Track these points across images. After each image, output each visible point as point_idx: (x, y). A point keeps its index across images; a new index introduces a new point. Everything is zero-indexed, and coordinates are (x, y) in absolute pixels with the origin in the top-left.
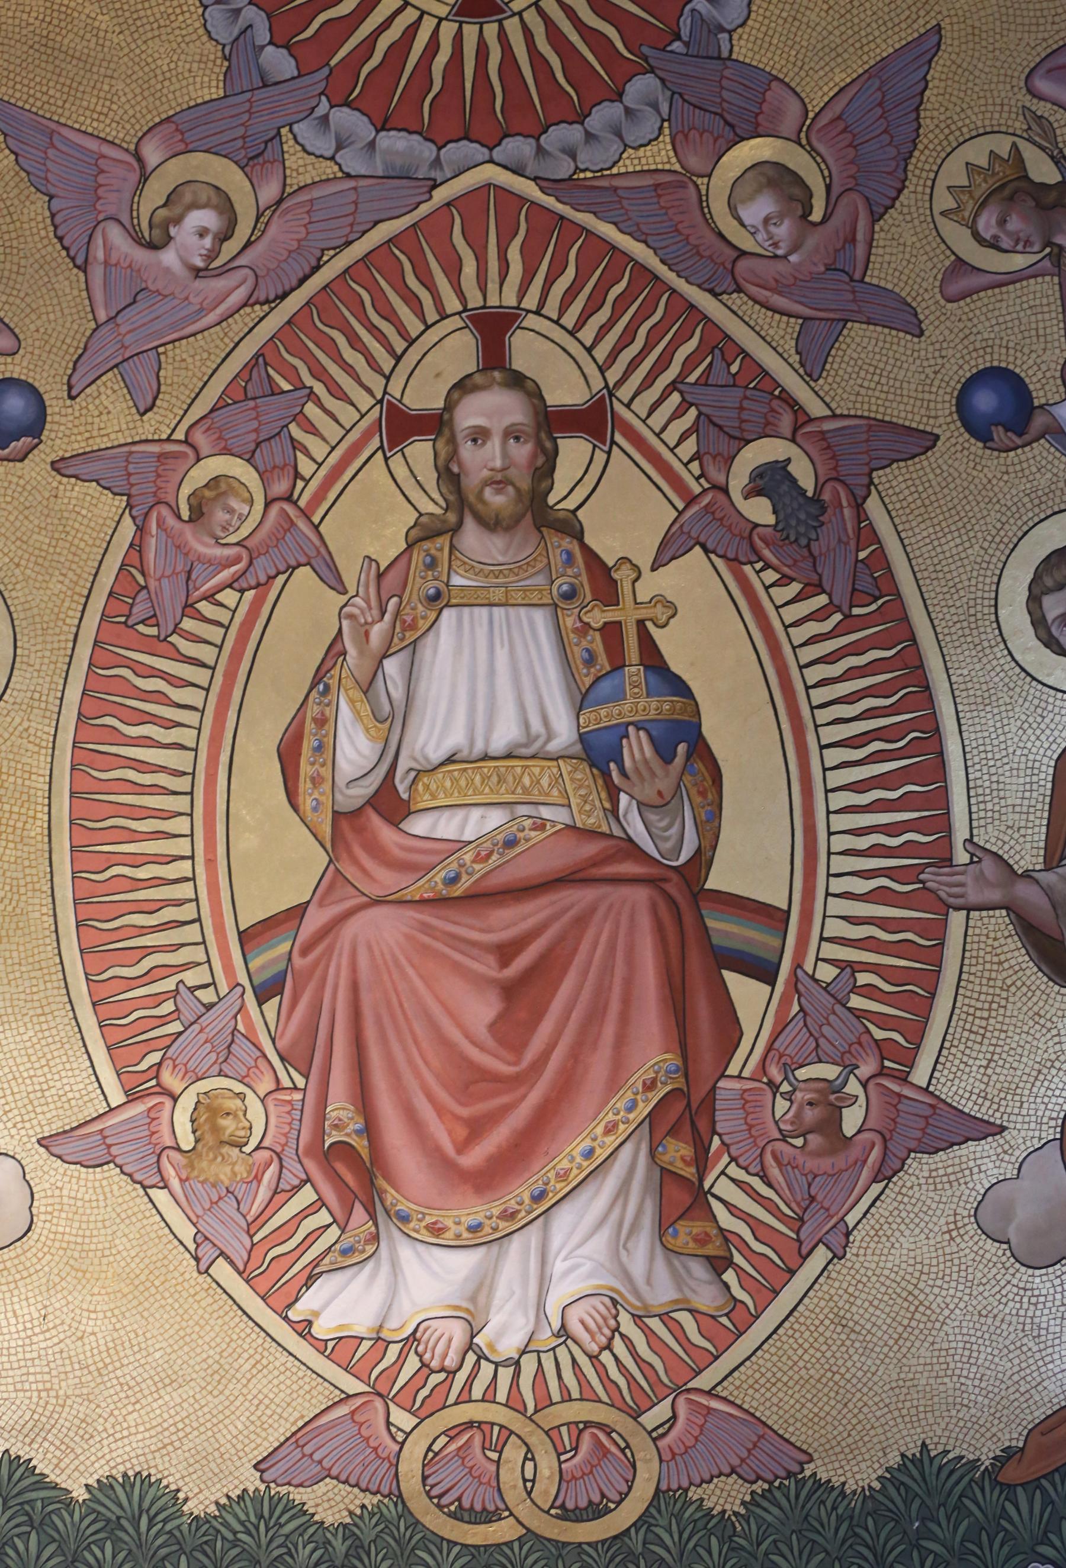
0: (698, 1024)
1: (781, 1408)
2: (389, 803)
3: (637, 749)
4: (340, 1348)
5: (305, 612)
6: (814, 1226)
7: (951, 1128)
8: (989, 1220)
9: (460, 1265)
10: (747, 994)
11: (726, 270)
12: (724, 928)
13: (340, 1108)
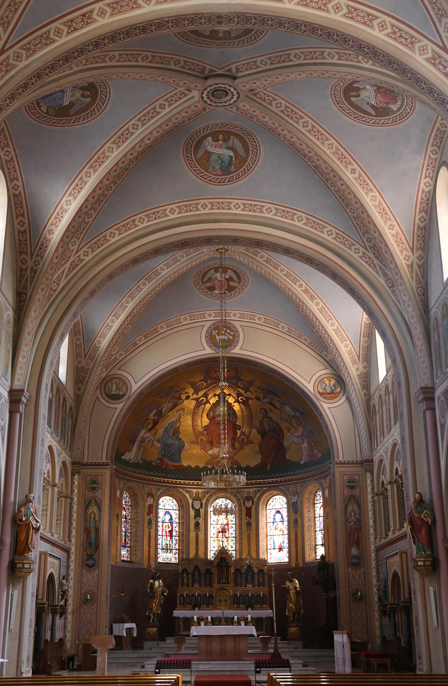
2: (214, 418)
3: (231, 414)
4: (210, 455)
5: (208, 406)
6: (242, 448)
7: (251, 442)
9: (218, 449)
10: (238, 431)
11: (240, 388)
12: (237, 427)
13: (210, 438)
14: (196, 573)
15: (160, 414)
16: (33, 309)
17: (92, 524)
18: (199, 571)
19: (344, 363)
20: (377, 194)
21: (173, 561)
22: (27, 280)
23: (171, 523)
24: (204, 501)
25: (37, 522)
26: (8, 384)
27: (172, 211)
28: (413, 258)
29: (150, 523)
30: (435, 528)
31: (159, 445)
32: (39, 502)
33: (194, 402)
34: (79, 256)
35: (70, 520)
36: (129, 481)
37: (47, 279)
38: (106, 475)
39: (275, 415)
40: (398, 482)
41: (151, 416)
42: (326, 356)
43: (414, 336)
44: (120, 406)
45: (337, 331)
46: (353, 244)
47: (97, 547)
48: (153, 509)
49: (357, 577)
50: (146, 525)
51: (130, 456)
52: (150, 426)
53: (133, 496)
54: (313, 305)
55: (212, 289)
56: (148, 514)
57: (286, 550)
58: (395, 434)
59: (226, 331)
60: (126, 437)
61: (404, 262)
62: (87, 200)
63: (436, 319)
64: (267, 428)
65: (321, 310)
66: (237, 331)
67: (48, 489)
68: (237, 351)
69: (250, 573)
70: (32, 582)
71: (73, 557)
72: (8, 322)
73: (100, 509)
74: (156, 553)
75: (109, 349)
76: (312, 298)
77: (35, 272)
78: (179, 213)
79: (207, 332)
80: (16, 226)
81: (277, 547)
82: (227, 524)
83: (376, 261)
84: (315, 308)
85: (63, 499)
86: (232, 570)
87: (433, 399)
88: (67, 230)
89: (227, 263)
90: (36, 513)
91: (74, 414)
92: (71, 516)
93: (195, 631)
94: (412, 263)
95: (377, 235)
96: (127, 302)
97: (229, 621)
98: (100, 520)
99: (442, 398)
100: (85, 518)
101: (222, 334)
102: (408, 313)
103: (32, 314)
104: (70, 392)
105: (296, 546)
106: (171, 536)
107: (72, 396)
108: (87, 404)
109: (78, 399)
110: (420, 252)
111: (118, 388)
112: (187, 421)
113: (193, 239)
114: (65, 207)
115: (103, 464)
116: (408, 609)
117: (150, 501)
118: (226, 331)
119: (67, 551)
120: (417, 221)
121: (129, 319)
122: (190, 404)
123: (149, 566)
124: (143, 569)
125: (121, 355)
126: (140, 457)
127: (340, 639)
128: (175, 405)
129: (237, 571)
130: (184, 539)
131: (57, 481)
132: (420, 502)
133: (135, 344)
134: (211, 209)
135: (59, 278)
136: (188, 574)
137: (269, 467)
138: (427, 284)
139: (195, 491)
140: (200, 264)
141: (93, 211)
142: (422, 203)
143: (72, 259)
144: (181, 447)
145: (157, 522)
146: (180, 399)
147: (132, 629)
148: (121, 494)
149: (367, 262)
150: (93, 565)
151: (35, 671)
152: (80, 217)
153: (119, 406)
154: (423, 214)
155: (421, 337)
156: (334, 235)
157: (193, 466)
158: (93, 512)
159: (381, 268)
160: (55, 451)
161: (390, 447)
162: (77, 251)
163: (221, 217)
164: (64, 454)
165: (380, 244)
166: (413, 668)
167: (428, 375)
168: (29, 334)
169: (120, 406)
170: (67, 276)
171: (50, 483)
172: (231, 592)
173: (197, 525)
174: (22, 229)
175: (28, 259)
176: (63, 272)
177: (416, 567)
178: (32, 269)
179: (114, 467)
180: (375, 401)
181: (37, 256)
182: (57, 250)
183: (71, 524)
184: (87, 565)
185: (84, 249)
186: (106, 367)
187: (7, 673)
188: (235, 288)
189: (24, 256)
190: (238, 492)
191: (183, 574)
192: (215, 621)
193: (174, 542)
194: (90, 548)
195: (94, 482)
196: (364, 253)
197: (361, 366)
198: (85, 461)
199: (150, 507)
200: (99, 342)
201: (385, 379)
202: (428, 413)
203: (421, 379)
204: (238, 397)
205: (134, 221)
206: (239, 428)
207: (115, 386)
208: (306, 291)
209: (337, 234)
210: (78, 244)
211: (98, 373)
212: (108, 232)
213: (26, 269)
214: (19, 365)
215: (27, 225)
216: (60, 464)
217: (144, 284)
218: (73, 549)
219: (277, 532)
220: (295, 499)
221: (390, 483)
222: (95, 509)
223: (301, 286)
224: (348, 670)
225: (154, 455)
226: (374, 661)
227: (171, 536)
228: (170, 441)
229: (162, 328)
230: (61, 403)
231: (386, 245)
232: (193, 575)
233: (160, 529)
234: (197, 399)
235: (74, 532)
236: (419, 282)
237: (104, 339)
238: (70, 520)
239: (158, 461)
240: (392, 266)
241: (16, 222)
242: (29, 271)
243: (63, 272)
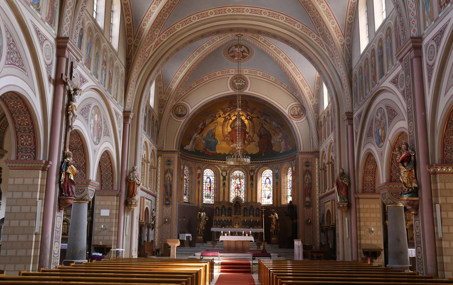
0: (245, 136)
1: (247, 151)
2: (234, 127)
5: (231, 121)
6: (249, 144)
7: (253, 141)
8: (255, 145)
14: (223, 209)
15: (204, 125)
16: (135, 67)
17: (168, 183)
18: (225, 208)
19: (305, 99)
20: (325, 4)
21: (211, 203)
22: (132, 51)
23: (210, 183)
24: (228, 172)
25: (139, 181)
26: (123, 108)
27: (211, 13)
28: (344, 41)
29: (199, 183)
30: (350, 187)
31: (204, 142)
32: (139, 171)
33: (223, 119)
34: (160, 38)
35: (156, 181)
36: (188, 160)
37: (143, 51)
38: (175, 157)
39: (267, 127)
40: (332, 163)
41: (200, 126)
42: (296, 94)
43: (343, 84)
44: (183, 121)
45: (302, 81)
46: (312, 33)
47: (171, 195)
48: (200, 176)
49: (308, 212)
50: (197, 184)
51: (188, 147)
52: (199, 132)
53: (190, 169)
54: (289, 66)
55: (234, 57)
56: (198, 178)
57: (271, 198)
58: (331, 137)
59: (241, 81)
60: (186, 138)
61: (339, 43)
62: (164, 7)
63: (355, 75)
64: (262, 134)
65: (293, 69)
66: (247, 80)
67: (145, 165)
68: (247, 91)
69: (252, 210)
70: (137, 211)
71: (158, 200)
72: (122, 75)
73: (172, 175)
74: (202, 199)
75: (177, 90)
76: (289, 62)
77: (136, 47)
78: (215, 14)
79: (231, 81)
80: (126, 21)
81: (267, 196)
82: (240, 184)
83: (324, 42)
84: (290, 68)
85: (153, 169)
86: (242, 208)
87: (352, 119)
88: (153, 24)
89: (242, 42)
90: (138, 176)
91: (158, 124)
92: (157, 178)
93: (222, 238)
94: (344, 44)
95: (324, 28)
96: (187, 64)
97: (240, 234)
98: (172, 181)
99: (357, 118)
100: (165, 180)
101: (239, 82)
102: (340, 71)
103: (135, 70)
104: (156, 112)
105: (277, 196)
106: (210, 190)
107: (157, 115)
108: (165, 119)
109: (161, 117)
110: (348, 37)
111: (182, 111)
112: (219, 129)
113: (223, 29)
114: (152, 11)
115: (174, 152)
116: (334, 229)
117: (199, 171)
118: (241, 81)
119: (155, 196)
120: (347, 20)
121: (188, 73)
122: (221, 120)
123: (199, 205)
124: (195, 207)
125: (183, 93)
126: (194, 148)
127: (297, 243)
128: (213, 120)
129: (245, 208)
130: (217, 191)
131: (149, 160)
132: (342, 174)
133: (191, 87)
134: (233, 12)
135: (149, 51)
136: (219, 210)
137: (263, 154)
138: (351, 55)
139: (223, 166)
140: (227, 43)
141: (167, 13)
142: (350, 9)
143: (156, 40)
144: (216, 143)
145: (203, 182)
146: (216, 117)
147: (190, 237)
148: (184, 168)
149: (319, 43)
150: (169, 204)
151: (139, 255)
152: (160, 16)
153: (183, 121)
154: (351, 16)
155: (347, 85)
156: (301, 28)
157: (222, 153)
158: (169, 176)
159: (326, 46)
160: (148, 144)
161: (329, 144)
162: (159, 36)
163: (238, 17)
164: (153, 146)
165: (326, 33)
166: (335, 258)
167: (350, 106)
168: (133, 81)
169: (183, 121)
170: (153, 49)
171: (145, 161)
172: (242, 219)
173: (224, 184)
174: (129, 23)
175: (133, 40)
176: (151, 47)
177: (339, 207)
178: (134, 45)
179: (180, 153)
180: (322, 120)
181: (137, 38)
182: (148, 35)
183: (157, 183)
184: (166, 204)
185: (163, 34)
186: (176, 99)
187: (125, 256)
188: (246, 56)
189: (130, 38)
190: (246, 167)
191: (216, 209)
192: (232, 234)
193: (212, 193)
194: (167, 195)
195: (169, 161)
196: (317, 38)
197: (314, 100)
198: (165, 149)
199: (199, 174)
200: (172, 86)
201: (327, 108)
202: (349, 126)
203: (346, 108)
204: (247, 116)
205: (190, 19)
206: (248, 133)
207: (180, 110)
208: (285, 59)
209: (303, 27)
210: (159, 32)
211: (171, 102)
212: (176, 25)
213: (131, 45)
214: (128, 98)
215: (131, 21)
216: (151, 151)
217: (196, 54)
218: (158, 196)
219: (267, 189)
220: (277, 171)
221: (328, 163)
222: (170, 175)
223: (282, 56)
224: (301, 258)
225: (201, 147)
226: (315, 255)
227: (210, 190)
228: (210, 140)
229: (206, 78)
230: (151, 118)
231: (330, 34)
232: (222, 210)
233: (204, 186)
234: (225, 118)
235: (159, 187)
236: (347, 54)
237: (174, 84)
238: (156, 181)
239: (204, 150)
240: (333, 45)
241: (126, 19)
242: (133, 46)
243: (151, 47)
